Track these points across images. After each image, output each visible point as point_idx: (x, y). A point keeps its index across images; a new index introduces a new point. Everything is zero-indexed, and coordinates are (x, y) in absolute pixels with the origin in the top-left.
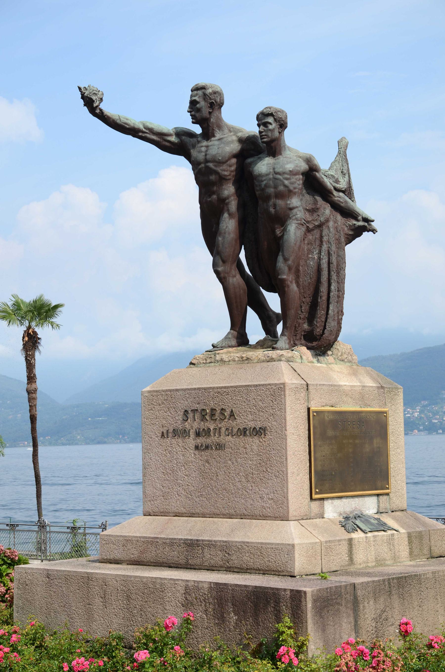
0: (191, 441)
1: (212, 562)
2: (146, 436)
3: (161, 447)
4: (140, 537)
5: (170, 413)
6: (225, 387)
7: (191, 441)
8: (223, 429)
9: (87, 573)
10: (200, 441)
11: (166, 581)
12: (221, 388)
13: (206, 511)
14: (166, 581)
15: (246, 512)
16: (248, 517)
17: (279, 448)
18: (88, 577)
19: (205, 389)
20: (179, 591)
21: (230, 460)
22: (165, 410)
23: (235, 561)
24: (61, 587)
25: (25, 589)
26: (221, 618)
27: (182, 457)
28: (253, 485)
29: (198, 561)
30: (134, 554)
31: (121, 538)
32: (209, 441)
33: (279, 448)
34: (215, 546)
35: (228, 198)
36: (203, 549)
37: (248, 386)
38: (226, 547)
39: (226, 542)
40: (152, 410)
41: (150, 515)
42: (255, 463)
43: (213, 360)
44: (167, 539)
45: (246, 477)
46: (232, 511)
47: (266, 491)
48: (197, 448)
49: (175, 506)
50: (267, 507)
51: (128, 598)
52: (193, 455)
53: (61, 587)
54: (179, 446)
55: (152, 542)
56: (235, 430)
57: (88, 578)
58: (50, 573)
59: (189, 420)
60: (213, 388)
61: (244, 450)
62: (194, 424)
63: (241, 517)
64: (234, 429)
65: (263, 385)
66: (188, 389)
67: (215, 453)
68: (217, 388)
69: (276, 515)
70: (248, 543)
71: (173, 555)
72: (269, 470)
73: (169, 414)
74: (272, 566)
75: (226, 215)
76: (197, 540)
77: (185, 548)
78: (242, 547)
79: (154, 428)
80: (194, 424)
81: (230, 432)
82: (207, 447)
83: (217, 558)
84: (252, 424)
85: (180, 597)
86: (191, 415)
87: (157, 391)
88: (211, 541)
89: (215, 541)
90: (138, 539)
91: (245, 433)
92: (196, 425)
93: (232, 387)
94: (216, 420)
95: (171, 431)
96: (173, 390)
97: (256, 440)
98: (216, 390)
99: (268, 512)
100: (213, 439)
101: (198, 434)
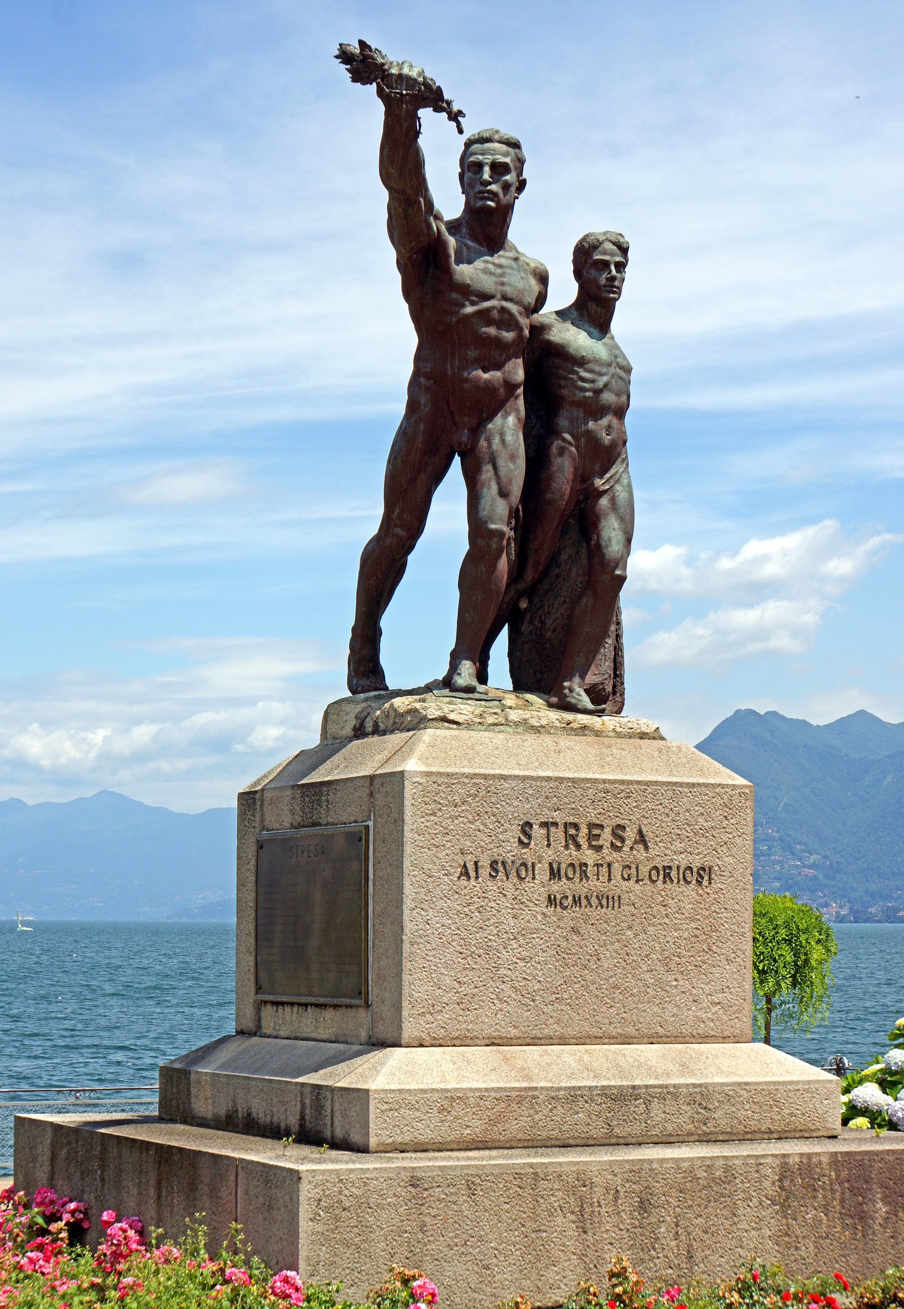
0: (538, 886)
1: (670, 1128)
2: (416, 873)
3: (456, 896)
4: (487, 1090)
5: (486, 826)
6: (622, 782)
7: (538, 886)
8: (617, 867)
9: (531, 1165)
10: (556, 888)
11: (736, 1162)
12: (615, 782)
13: (571, 1032)
14: (736, 1162)
15: (661, 1031)
16: (664, 1039)
17: (737, 907)
18: (536, 1174)
19: (573, 781)
20: (766, 1177)
21: (630, 928)
22: (470, 817)
23: (721, 1119)
24: (454, 1203)
25: (337, 1218)
26: (860, 1217)
27: (512, 922)
28: (679, 976)
29: (637, 1129)
30: (475, 1127)
31: (436, 1096)
32: (580, 888)
33: (737, 907)
34: (675, 1096)
35: (517, 386)
36: (647, 1103)
37: (675, 784)
38: (701, 1097)
39: (700, 1085)
40: (434, 814)
41: (422, 1046)
42: (686, 935)
43: (501, 720)
44: (559, 1089)
45: (666, 962)
46: (631, 1030)
47: (707, 988)
48: (551, 901)
49: (489, 1021)
50: (709, 1018)
51: (644, 1206)
52: (539, 917)
53: (454, 1203)
54: (505, 896)
55: (525, 1097)
56: (644, 870)
57: (537, 1175)
58: (419, 1174)
59: (533, 843)
60: (595, 781)
61: (663, 909)
62: (546, 851)
63: (651, 1040)
64: (641, 867)
65: (706, 785)
66: (532, 778)
67: (595, 913)
68: (604, 781)
69: (726, 1033)
70: (747, 1084)
71: (579, 1120)
72: (714, 948)
73: (481, 827)
74: (799, 1122)
75: (511, 420)
76: (634, 1087)
77: (603, 1105)
78: (732, 1094)
79: (440, 855)
80: (546, 851)
81: (630, 872)
82: (577, 901)
83: (683, 1118)
84: (682, 861)
85: (769, 1188)
86: (538, 832)
87: (448, 775)
88: (667, 1087)
89: (675, 1086)
90: (482, 1095)
91: (667, 876)
92: (549, 855)
93: (638, 782)
94: (601, 847)
95: (485, 862)
96: (494, 777)
97: (691, 891)
98: (601, 786)
99: (709, 1028)
100: (595, 885)
101: (554, 873)
